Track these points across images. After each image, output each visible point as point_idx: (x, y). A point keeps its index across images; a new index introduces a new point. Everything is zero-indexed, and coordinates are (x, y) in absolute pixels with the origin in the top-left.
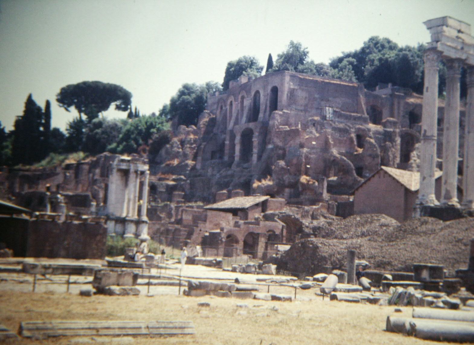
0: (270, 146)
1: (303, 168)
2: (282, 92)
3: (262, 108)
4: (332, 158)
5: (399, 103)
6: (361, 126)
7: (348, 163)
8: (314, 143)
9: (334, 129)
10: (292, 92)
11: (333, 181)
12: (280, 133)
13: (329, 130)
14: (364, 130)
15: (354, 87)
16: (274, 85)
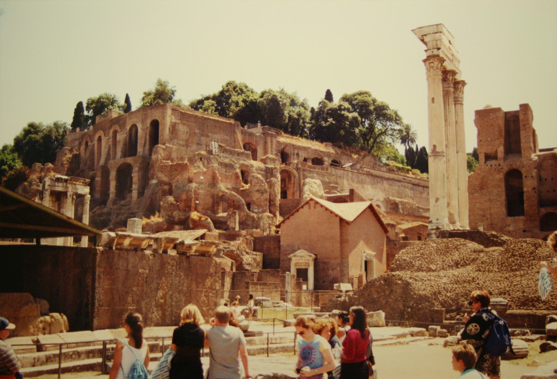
0: (154, 181)
1: (193, 205)
2: (164, 125)
3: (140, 142)
4: (221, 194)
5: (272, 142)
6: (244, 162)
7: (239, 199)
8: (202, 178)
9: (221, 164)
10: (174, 127)
11: (223, 217)
12: (163, 168)
13: (216, 165)
14: (247, 166)
15: (231, 124)
16: (155, 118)
